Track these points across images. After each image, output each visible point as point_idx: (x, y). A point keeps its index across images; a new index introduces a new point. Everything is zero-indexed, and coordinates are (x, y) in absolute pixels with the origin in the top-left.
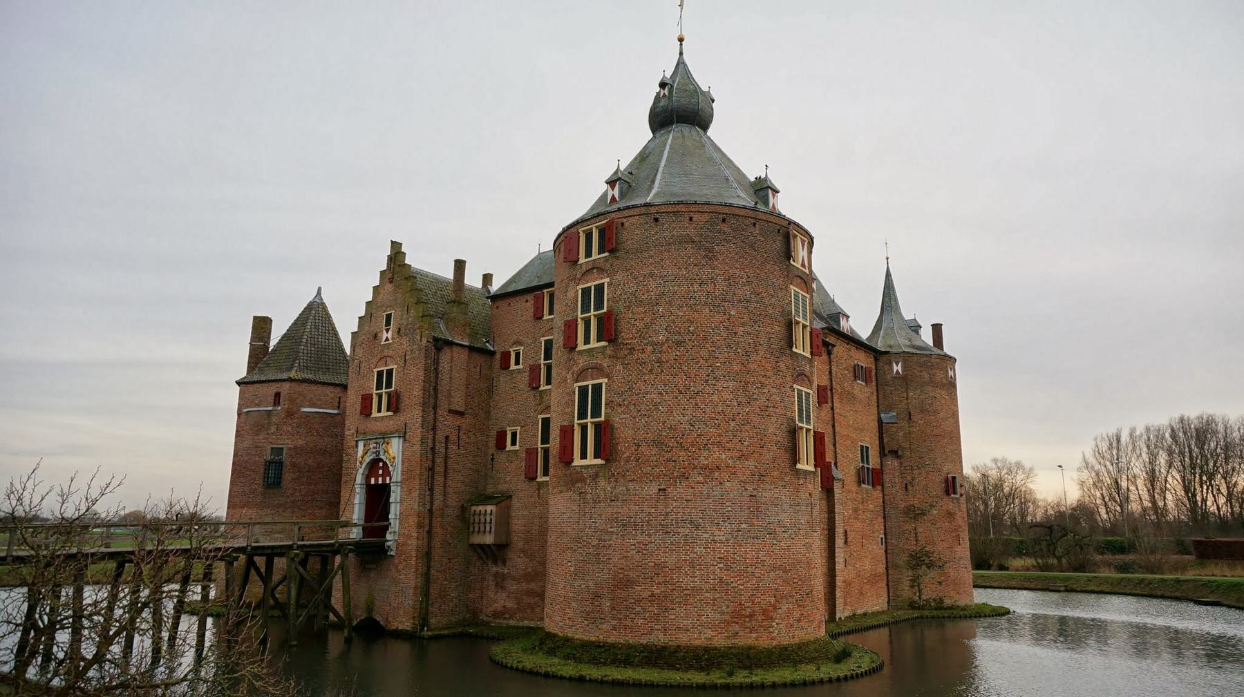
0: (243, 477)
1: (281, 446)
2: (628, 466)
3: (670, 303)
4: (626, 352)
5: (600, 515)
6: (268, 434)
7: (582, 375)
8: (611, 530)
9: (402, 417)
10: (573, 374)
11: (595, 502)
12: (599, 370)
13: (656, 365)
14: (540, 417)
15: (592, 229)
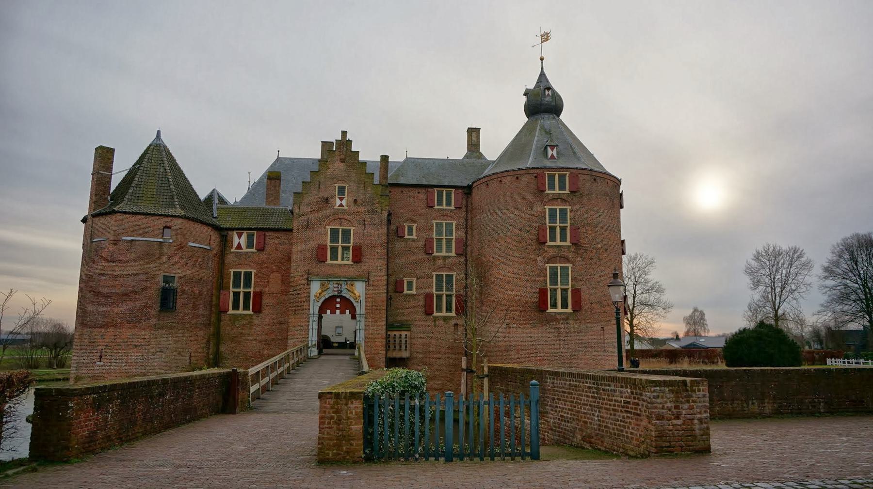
0: (131, 300)
1: (172, 275)
2: (586, 315)
3: (602, 228)
4: (583, 251)
5: (571, 341)
6: (160, 263)
7: (552, 259)
8: (579, 349)
9: (362, 269)
10: (544, 258)
11: (567, 333)
12: (566, 260)
13: (598, 260)
14: (434, 274)
15: (555, 174)
